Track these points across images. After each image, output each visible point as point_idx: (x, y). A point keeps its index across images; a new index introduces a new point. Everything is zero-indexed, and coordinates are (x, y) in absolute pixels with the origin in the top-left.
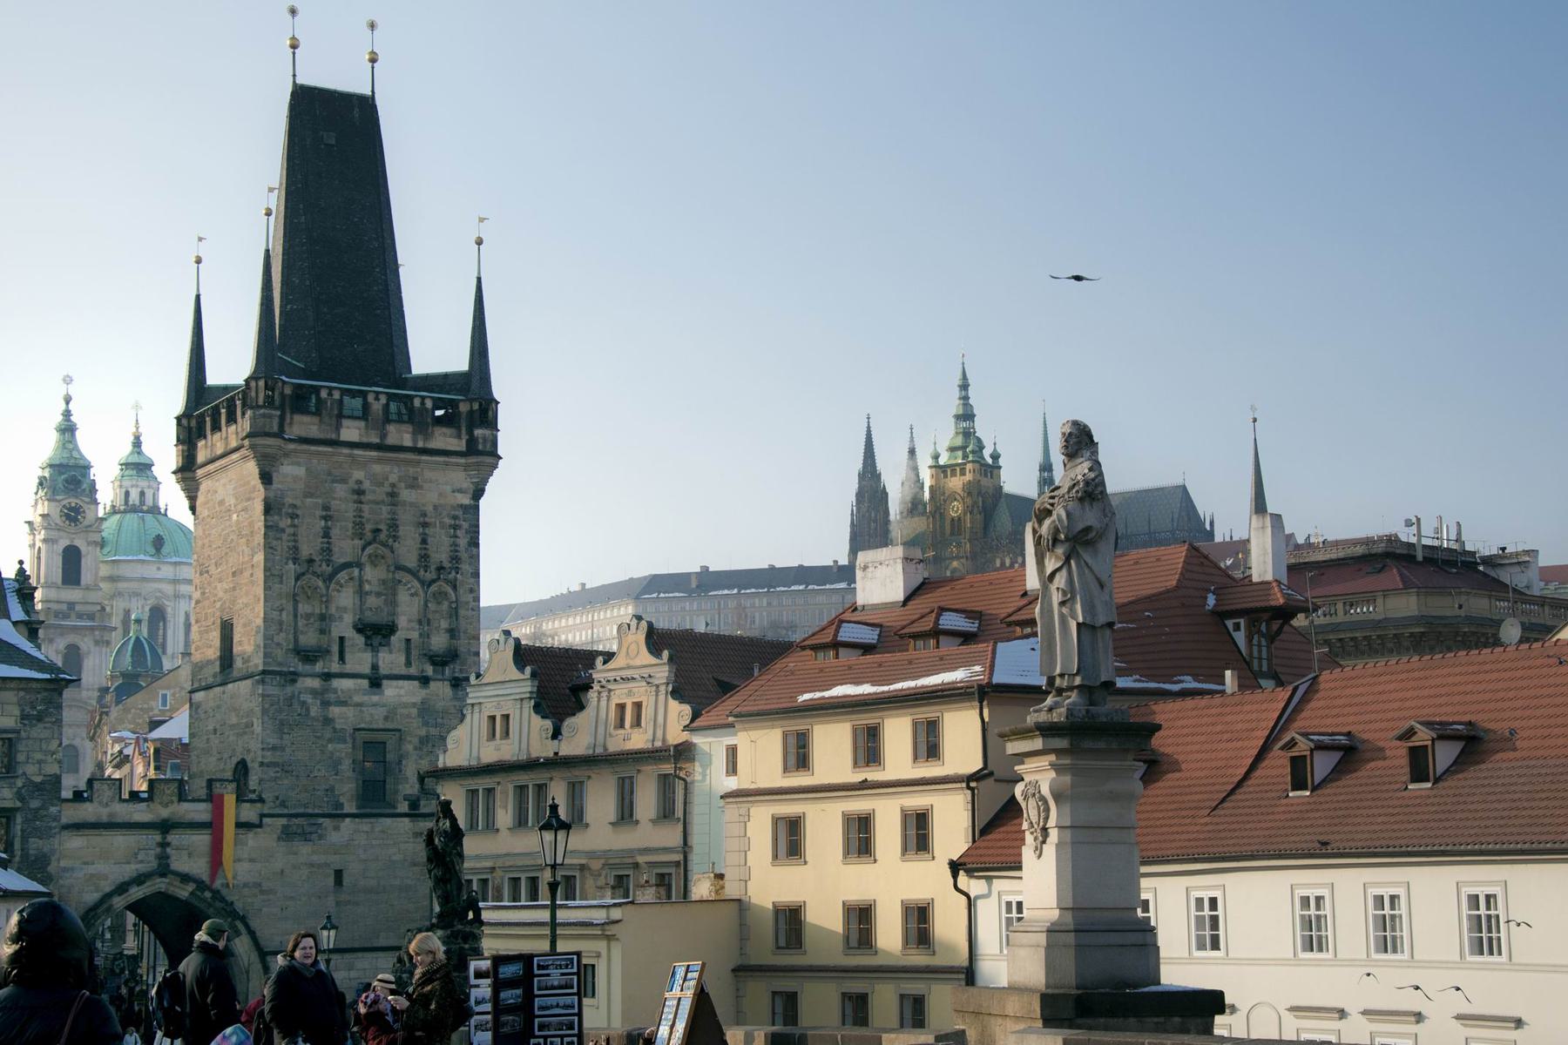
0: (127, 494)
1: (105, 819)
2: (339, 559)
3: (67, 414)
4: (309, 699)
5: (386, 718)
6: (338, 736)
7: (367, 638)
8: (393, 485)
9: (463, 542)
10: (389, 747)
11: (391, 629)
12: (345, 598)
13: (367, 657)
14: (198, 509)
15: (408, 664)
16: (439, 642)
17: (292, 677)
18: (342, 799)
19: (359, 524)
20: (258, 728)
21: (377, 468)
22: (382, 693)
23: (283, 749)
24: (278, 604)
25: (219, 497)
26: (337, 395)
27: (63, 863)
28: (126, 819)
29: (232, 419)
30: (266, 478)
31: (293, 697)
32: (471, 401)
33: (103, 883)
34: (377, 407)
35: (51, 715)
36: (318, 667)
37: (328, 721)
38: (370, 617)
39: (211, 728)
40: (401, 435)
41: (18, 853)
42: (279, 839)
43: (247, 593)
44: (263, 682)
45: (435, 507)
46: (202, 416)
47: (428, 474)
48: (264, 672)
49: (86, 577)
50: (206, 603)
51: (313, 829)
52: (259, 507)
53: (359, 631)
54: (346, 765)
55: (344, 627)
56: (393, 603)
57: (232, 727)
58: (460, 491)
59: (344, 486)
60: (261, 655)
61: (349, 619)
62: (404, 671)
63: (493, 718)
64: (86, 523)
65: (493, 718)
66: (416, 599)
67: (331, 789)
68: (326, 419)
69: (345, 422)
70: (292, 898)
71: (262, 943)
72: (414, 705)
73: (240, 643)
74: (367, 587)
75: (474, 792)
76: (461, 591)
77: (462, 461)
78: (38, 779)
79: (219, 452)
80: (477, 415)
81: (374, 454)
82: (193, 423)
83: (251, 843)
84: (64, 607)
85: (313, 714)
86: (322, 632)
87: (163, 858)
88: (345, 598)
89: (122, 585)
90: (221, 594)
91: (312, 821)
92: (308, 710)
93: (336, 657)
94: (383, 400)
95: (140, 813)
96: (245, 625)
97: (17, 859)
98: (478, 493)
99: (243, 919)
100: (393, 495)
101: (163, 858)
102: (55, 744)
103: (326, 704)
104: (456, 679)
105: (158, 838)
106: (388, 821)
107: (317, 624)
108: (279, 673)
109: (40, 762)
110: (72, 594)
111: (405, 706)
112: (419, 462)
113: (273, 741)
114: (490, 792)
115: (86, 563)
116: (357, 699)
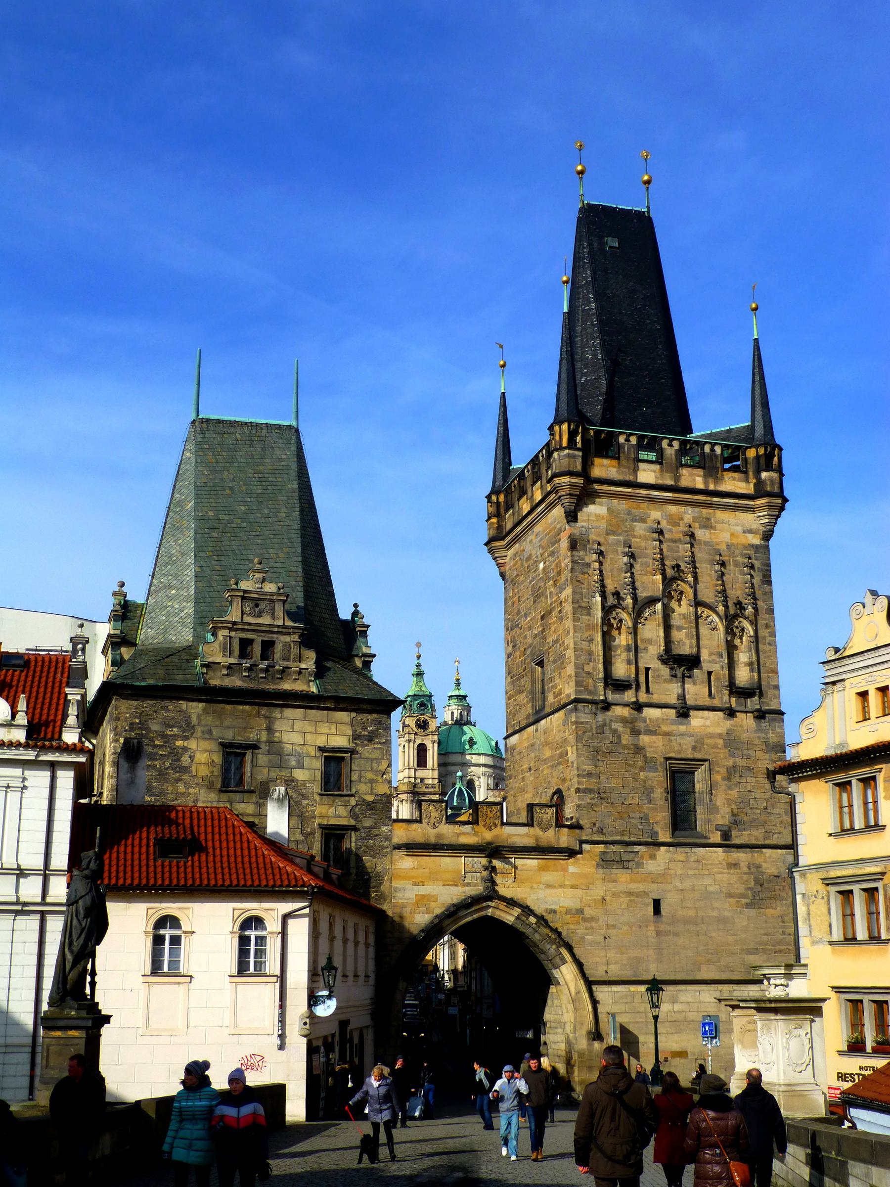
0: (452, 713)
1: (433, 840)
2: (643, 594)
3: (419, 665)
5: (694, 748)
6: (648, 763)
7: (672, 669)
9: (757, 580)
10: (698, 775)
11: (693, 662)
18: (657, 828)
20: (572, 755)
21: (673, 509)
22: (689, 723)
24: (587, 634)
25: (526, 555)
26: (634, 440)
27: (395, 883)
28: (453, 840)
29: (537, 477)
30: (572, 516)
31: (604, 724)
32: (757, 447)
33: (433, 904)
34: (670, 449)
35: (381, 736)
37: (639, 750)
39: (525, 767)
40: (694, 478)
41: (353, 871)
42: (598, 866)
43: (555, 632)
44: (576, 709)
46: (510, 486)
47: (720, 515)
48: (576, 701)
49: (430, 763)
50: (517, 654)
52: (564, 544)
53: (664, 662)
55: (651, 657)
57: (545, 761)
58: (750, 531)
59: (643, 525)
60: (572, 684)
62: (707, 702)
63: (864, 695)
64: (430, 730)
65: (864, 695)
67: (645, 818)
68: (624, 462)
69: (641, 465)
70: (614, 927)
71: (587, 972)
72: (720, 736)
73: (552, 679)
75: (844, 786)
78: (370, 798)
79: (525, 507)
80: (762, 461)
81: (670, 495)
82: (502, 498)
83: (572, 869)
84: (418, 781)
85: (624, 742)
86: (629, 662)
89: (451, 768)
90: (530, 640)
91: (630, 849)
92: (619, 737)
94: (676, 445)
95: (467, 835)
96: (555, 661)
97: (353, 877)
98: (768, 536)
102: (385, 764)
103: (636, 732)
106: (702, 850)
107: (624, 656)
108: (593, 702)
109: (372, 781)
110: (421, 773)
111: (712, 736)
113: (588, 768)
114: (868, 782)
115: (429, 754)
116: (665, 728)
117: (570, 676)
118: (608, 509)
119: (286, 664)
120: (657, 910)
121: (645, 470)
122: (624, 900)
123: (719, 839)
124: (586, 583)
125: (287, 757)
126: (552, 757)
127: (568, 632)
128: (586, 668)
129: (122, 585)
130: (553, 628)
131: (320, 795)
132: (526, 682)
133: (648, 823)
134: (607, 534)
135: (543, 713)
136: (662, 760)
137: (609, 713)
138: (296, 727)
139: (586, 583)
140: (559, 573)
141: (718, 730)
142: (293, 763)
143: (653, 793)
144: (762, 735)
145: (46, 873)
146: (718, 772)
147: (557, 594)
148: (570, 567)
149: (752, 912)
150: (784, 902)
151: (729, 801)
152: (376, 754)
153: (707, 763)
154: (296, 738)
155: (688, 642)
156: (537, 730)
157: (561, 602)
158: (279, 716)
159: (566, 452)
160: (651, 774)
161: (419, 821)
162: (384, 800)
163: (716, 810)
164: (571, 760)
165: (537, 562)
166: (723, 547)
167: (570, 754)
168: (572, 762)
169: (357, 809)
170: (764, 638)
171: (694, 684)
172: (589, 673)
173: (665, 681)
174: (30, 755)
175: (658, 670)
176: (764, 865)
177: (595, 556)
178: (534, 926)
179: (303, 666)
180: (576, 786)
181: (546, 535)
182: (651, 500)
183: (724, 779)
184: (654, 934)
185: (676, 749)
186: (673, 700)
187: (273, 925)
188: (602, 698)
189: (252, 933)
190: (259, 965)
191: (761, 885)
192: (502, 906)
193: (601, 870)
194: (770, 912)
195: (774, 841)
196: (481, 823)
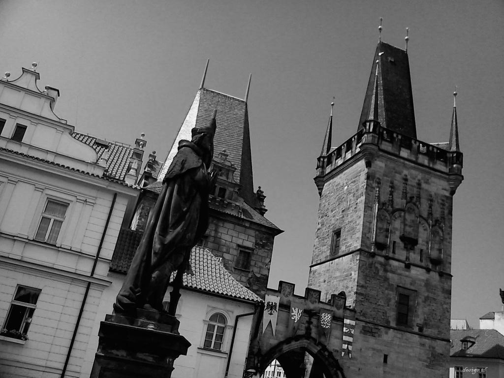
4: (379, 266)
5: (411, 284)
6: (390, 287)
7: (405, 244)
8: (419, 180)
9: (446, 212)
10: (411, 298)
12: (397, 224)
13: (404, 253)
14: (323, 193)
15: (421, 260)
16: (434, 254)
17: (373, 255)
18: (390, 319)
19: (405, 194)
20: (355, 275)
21: (414, 172)
22: (410, 271)
23: (366, 288)
26: (400, 137)
30: (368, 165)
35: (268, 246)
36: (384, 253)
37: (386, 279)
38: (406, 235)
39: (322, 280)
43: (351, 217)
45: (435, 194)
47: (433, 179)
51: (376, 331)
54: (393, 302)
55: (396, 237)
56: (418, 232)
58: (445, 190)
60: (360, 242)
61: (398, 234)
66: (426, 232)
67: (385, 313)
69: (402, 149)
72: (423, 280)
74: (407, 223)
76: (444, 233)
77: (447, 177)
78: (259, 276)
79: (340, 162)
80: (455, 159)
81: (413, 165)
82: (326, 160)
85: (380, 274)
87: (308, 329)
88: (397, 224)
91: (376, 327)
92: (378, 271)
93: (391, 250)
96: (349, 231)
98: (453, 192)
99: (341, 370)
100: (419, 184)
101: (308, 329)
104: (441, 272)
105: (307, 319)
106: (409, 335)
109: (260, 268)
111: (420, 280)
112: (430, 173)
113: (362, 283)
116: (399, 271)
117: (358, 238)
118: (386, 165)
119: (229, 201)
120: (385, 361)
121: (403, 151)
122: (370, 353)
123: (418, 330)
124: (372, 195)
125: (222, 246)
126: (340, 276)
127: (360, 217)
128: (367, 235)
129: (154, 153)
130: (349, 216)
131: (234, 268)
132: (329, 241)
133: (386, 316)
134: (385, 175)
135: (337, 256)
136: (396, 286)
137: (375, 259)
138: (229, 233)
139: (372, 195)
140: (357, 190)
141: (423, 278)
142: (224, 250)
143: (390, 302)
144: (441, 284)
145: (97, 259)
146: (420, 298)
147: (354, 200)
148: (365, 187)
149: (429, 370)
150: (444, 368)
151: (424, 313)
152: (265, 255)
153: (415, 292)
154: (228, 238)
155: (413, 234)
156: (332, 263)
157: (357, 204)
158: (222, 225)
159: (371, 134)
160: (391, 292)
161: (280, 292)
162: (265, 278)
163: (418, 316)
164: (353, 278)
165: (343, 187)
166: (433, 194)
167: (353, 275)
168: (354, 279)
169: (251, 280)
170: (447, 239)
171: (414, 253)
172: (368, 238)
173: (401, 249)
174: (104, 184)
175: (399, 243)
176: (437, 348)
177: (377, 185)
178: (327, 357)
179: (237, 204)
180: (356, 291)
181: (351, 174)
182: (405, 166)
183: (423, 302)
184: (382, 372)
185: (403, 282)
186: (403, 258)
187: (231, 322)
188: (372, 250)
189: (217, 325)
190: (218, 345)
191: (434, 357)
192: (313, 344)
193: (362, 335)
194: (437, 372)
195: (442, 336)
196: (309, 300)
